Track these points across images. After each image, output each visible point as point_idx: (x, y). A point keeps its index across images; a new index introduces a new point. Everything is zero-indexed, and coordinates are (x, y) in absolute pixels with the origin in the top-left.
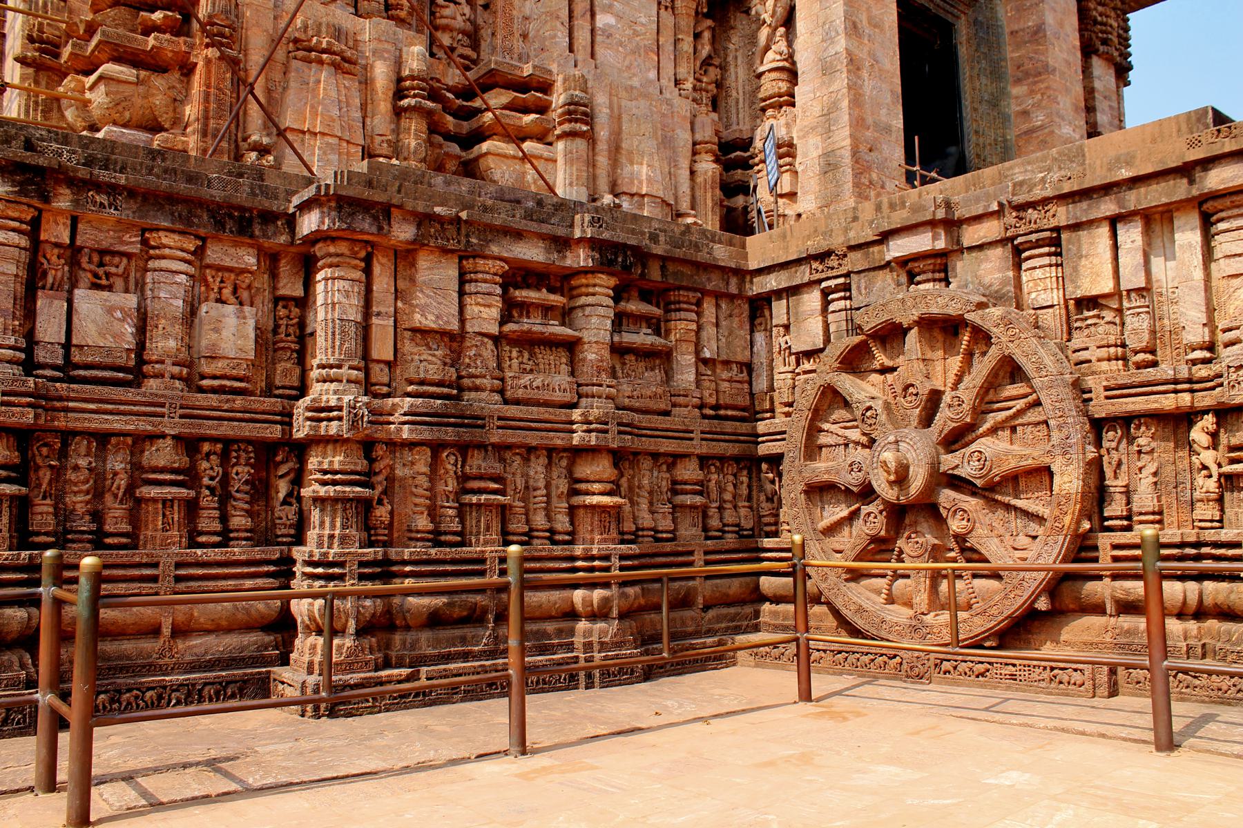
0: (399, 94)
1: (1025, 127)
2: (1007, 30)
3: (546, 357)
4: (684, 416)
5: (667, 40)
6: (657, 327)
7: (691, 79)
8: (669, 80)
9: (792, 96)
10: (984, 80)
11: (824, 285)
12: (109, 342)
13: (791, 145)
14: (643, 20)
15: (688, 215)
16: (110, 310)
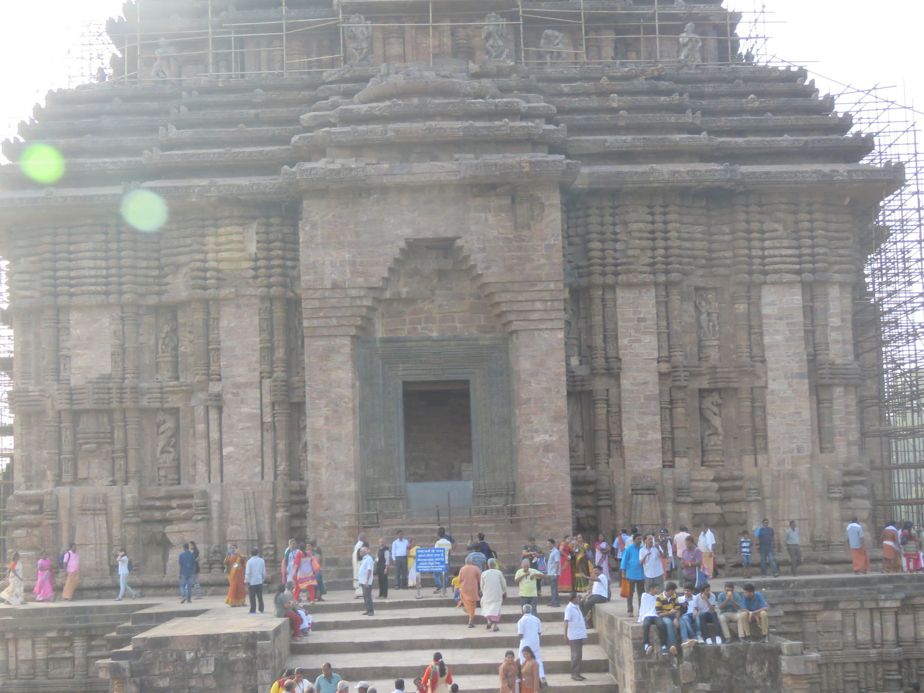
8: (269, 469)
14: (252, 442)
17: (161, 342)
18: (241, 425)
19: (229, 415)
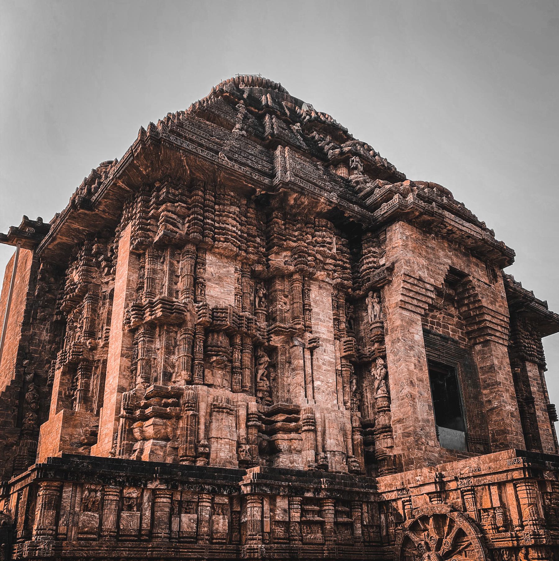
0: (248, 420)
1: (490, 407)
2: (478, 367)
3: (315, 528)
4: (359, 546)
5: (340, 387)
6: (349, 515)
7: (350, 402)
9: (389, 407)
10: (470, 389)
11: (403, 499)
12: (190, 530)
13: (390, 427)
14: (331, 381)
15: (352, 457)
16: (190, 520)
17: (257, 300)
18: (324, 367)
19: (318, 358)
